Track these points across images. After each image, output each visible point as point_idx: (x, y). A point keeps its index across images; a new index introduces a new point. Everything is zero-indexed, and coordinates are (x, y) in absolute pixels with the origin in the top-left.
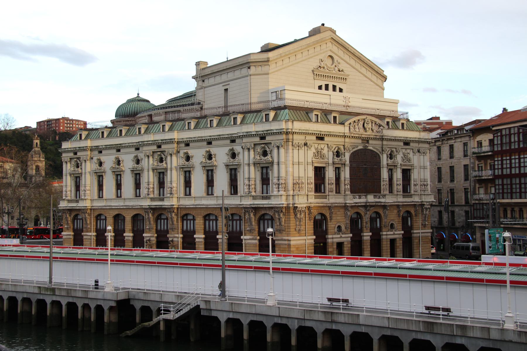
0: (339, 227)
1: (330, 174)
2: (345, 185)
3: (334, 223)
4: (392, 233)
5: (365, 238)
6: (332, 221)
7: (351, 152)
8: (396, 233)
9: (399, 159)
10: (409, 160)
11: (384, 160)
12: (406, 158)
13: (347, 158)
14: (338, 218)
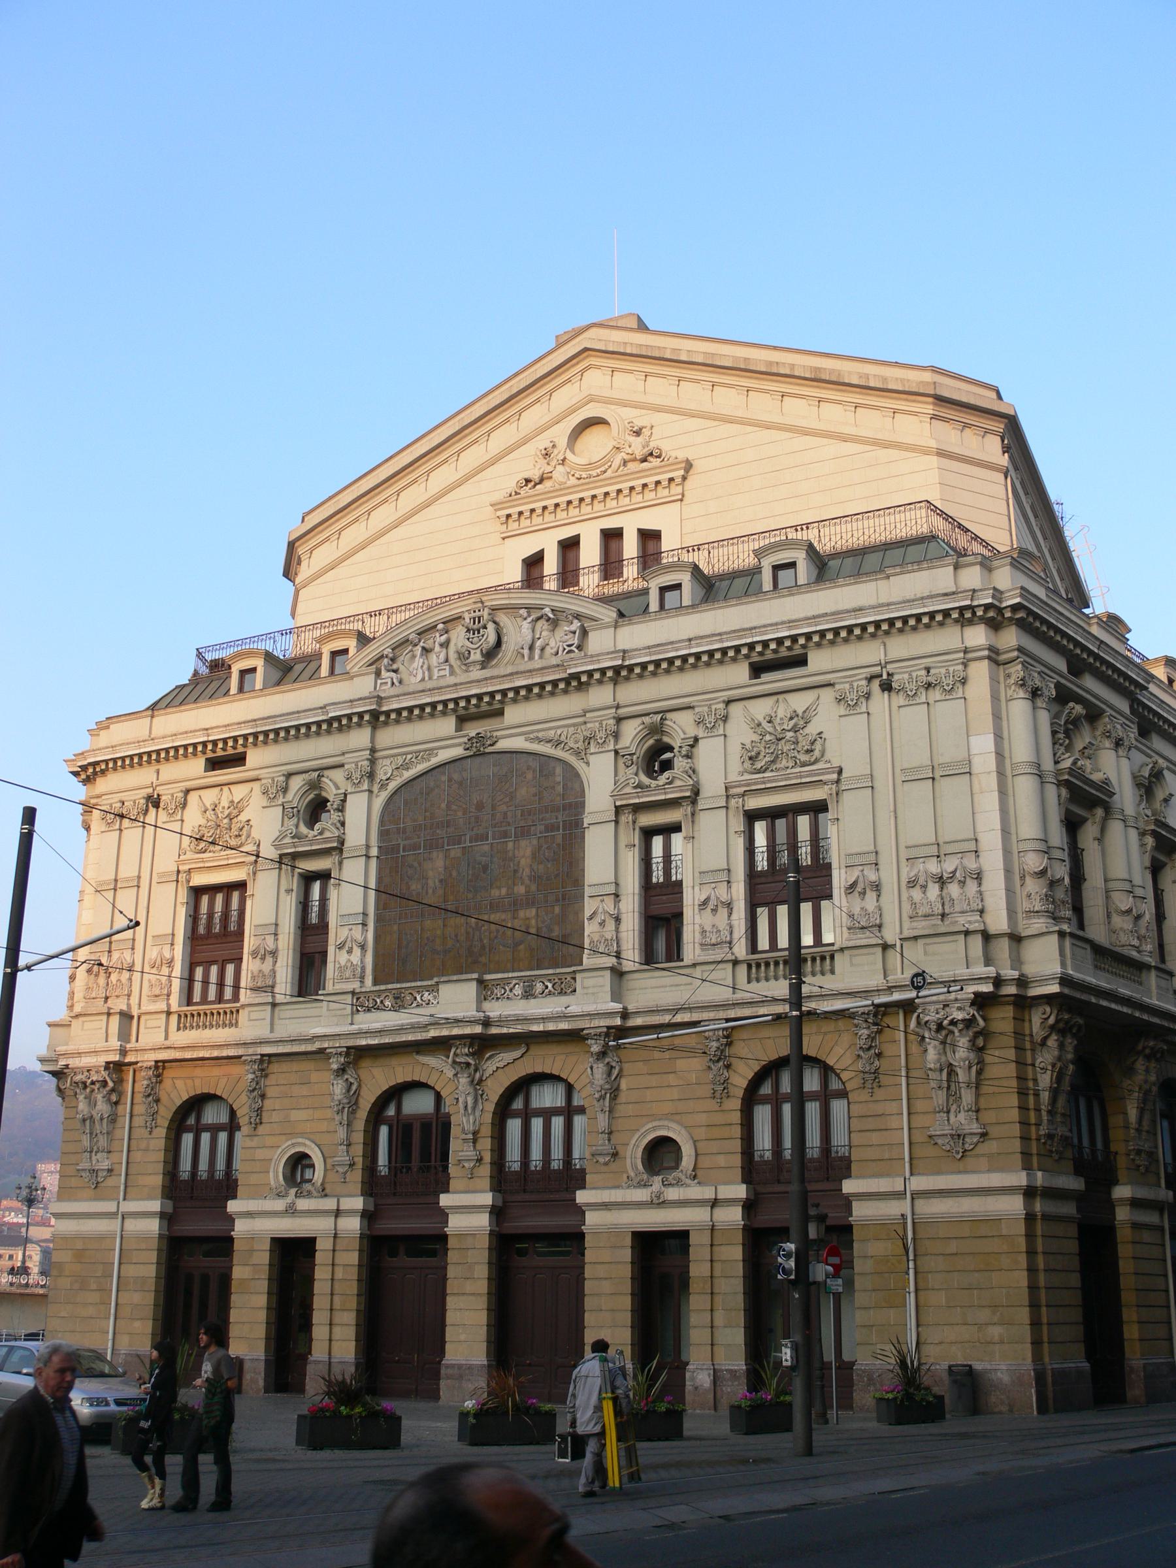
0: (299, 1161)
1: (269, 909)
2: (349, 956)
3: (270, 1141)
4: (642, 1195)
5: (456, 1223)
6: (261, 1129)
7: (392, 786)
8: (672, 1194)
9: (716, 764)
10: (813, 750)
11: (601, 781)
12: (784, 744)
13: (359, 819)
14: (296, 1115)
